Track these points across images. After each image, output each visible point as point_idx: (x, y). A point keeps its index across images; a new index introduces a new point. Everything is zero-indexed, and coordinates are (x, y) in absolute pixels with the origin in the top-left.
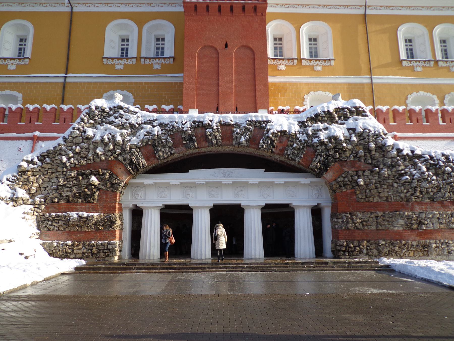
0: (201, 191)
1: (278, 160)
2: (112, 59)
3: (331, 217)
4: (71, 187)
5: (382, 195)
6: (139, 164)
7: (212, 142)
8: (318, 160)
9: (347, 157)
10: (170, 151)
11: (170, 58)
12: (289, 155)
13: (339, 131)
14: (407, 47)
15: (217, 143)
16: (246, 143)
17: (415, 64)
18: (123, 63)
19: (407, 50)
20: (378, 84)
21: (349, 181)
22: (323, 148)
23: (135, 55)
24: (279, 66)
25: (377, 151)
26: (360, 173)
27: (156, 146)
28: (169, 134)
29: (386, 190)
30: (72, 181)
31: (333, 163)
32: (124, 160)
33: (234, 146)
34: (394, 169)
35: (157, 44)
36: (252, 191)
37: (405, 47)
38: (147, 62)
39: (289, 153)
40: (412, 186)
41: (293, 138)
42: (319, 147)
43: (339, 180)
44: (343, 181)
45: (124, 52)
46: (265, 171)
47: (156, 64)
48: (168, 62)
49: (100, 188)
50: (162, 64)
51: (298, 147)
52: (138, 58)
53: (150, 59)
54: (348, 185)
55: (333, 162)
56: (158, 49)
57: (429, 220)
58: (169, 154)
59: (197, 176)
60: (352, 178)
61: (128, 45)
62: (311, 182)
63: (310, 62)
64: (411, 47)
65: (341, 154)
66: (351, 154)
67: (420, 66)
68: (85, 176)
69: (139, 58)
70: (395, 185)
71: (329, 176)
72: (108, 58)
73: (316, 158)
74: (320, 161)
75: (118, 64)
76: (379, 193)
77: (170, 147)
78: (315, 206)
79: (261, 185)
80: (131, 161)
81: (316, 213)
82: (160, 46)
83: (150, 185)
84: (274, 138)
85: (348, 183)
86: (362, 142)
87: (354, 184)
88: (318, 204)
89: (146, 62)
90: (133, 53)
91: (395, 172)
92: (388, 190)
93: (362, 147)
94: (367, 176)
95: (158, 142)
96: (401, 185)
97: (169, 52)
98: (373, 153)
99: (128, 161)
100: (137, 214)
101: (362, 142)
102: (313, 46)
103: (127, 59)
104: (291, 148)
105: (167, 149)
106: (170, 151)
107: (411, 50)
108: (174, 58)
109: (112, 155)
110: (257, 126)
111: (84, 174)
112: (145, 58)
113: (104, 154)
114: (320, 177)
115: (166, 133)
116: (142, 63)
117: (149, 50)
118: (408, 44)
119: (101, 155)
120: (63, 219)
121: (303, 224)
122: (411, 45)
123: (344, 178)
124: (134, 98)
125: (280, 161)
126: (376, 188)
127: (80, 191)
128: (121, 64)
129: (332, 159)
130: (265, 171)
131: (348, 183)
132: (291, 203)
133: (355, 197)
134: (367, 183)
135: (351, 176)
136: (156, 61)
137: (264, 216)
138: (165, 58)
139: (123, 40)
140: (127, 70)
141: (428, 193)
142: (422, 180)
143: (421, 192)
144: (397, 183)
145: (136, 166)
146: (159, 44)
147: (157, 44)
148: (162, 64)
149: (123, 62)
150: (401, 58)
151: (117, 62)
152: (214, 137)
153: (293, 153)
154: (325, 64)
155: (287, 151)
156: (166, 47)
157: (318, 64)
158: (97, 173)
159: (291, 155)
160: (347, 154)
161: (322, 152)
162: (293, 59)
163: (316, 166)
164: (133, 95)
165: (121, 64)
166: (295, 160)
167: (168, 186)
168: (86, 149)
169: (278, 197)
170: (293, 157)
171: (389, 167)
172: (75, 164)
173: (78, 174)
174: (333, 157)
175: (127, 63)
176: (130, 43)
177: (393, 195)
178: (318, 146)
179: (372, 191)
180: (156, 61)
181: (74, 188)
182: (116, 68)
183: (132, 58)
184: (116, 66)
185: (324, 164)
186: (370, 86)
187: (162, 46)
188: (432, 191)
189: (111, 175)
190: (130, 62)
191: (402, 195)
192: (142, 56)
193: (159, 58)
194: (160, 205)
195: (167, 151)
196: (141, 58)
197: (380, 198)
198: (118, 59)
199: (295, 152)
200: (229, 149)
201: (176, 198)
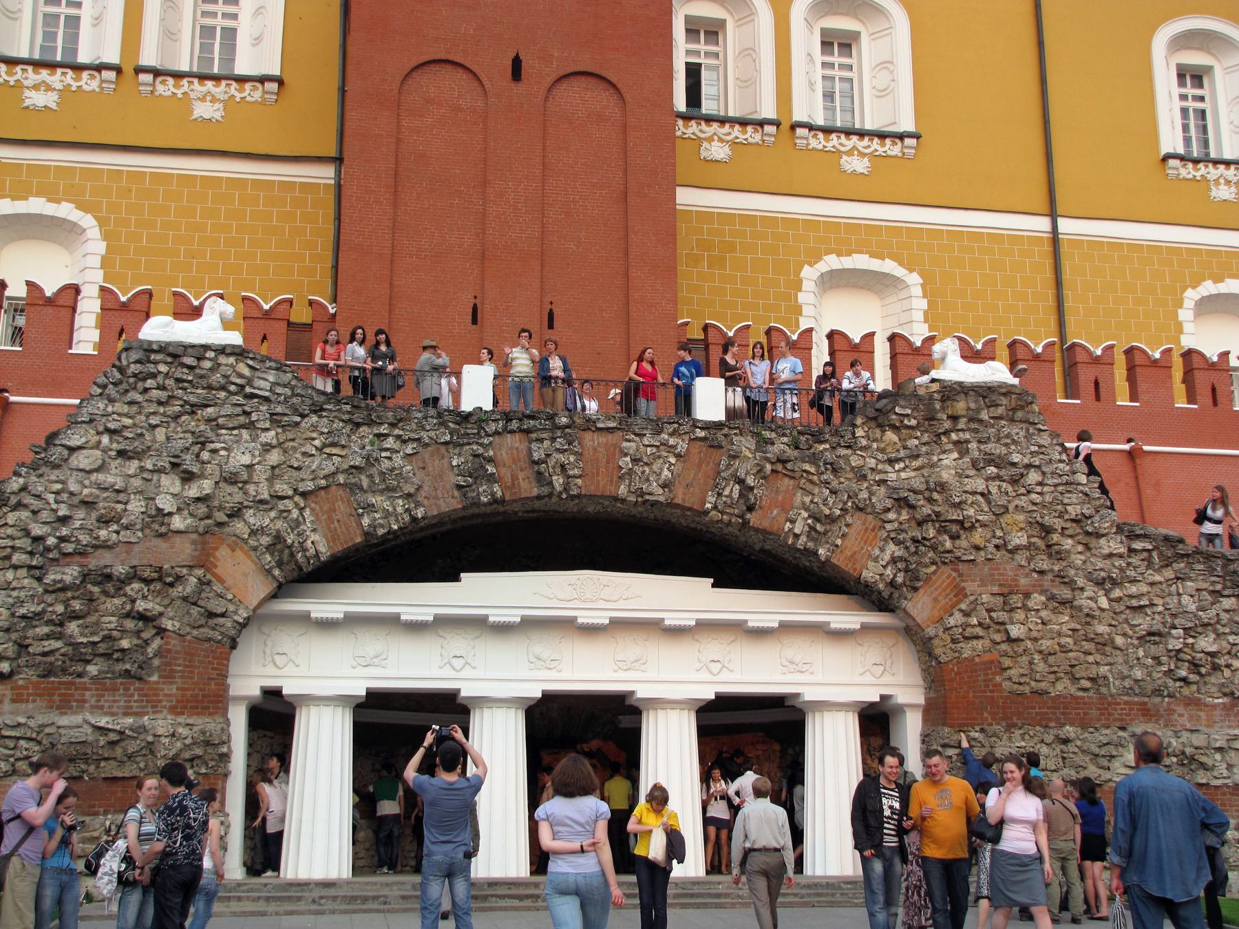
0: (499, 647)
1: (757, 547)
3: (923, 742)
4: (61, 624)
5: (1079, 672)
6: (305, 550)
7: (551, 483)
8: (887, 557)
9: (977, 548)
10: (408, 510)
11: (262, 80)
12: (797, 536)
14: (1185, 104)
15: (566, 489)
16: (661, 491)
17: (1213, 172)
18: (59, 86)
19: (1184, 111)
20: (1077, 243)
21: (980, 624)
22: (905, 516)
23: (113, 58)
24: (705, 144)
25: (1067, 532)
26: (1016, 600)
27: (361, 488)
28: (409, 451)
29: (1091, 659)
30: (66, 603)
31: (934, 568)
32: (253, 533)
33: (623, 501)
34: (1117, 593)
35: (204, 14)
36: (672, 649)
37: (1178, 104)
38: (166, 88)
39: (797, 531)
40: (1170, 647)
41: (811, 482)
42: (891, 516)
43: (952, 621)
44: (965, 626)
46: (714, 586)
47: (203, 99)
48: (257, 95)
49: (165, 630)
50: (229, 103)
51: (827, 512)
53: (178, 76)
54: (977, 637)
55: (933, 563)
56: (207, 32)
57: (1218, 756)
58: (407, 518)
59: (482, 591)
60: (991, 618)
62: (865, 628)
63: (827, 140)
64: (1199, 105)
65: (958, 537)
66: (989, 541)
67: (1228, 182)
68: (110, 587)
69: (128, 70)
70: (1119, 641)
71: (920, 607)
73: (882, 550)
74: (894, 560)
75: (36, 87)
76: (1072, 666)
77: (409, 495)
78: (872, 705)
79: (706, 627)
80: (278, 538)
81: (876, 723)
82: (220, 22)
83: (327, 625)
84: (750, 481)
85: (979, 631)
86: (1023, 502)
87: (998, 637)
88: (883, 697)
89: (160, 89)
91: (1119, 600)
92: (1098, 658)
93: (1021, 517)
94: (1038, 610)
95: (371, 476)
96: (1136, 642)
97: (259, 52)
98: (1055, 537)
99: (265, 540)
100: (274, 721)
101: (1023, 502)
102: (837, 73)
104: (806, 515)
105: (400, 502)
106: (408, 510)
107: (1202, 114)
108: (280, 81)
109: (208, 517)
110: (697, 439)
111: (109, 577)
112: (157, 73)
113: (179, 510)
114: (892, 611)
115: (397, 446)
118: (1190, 91)
119: (170, 514)
120: (34, 735)
121: (833, 761)
122: (1202, 99)
123: (967, 614)
124: (106, 237)
125: (762, 551)
126: (1065, 650)
127: (96, 639)
128: (49, 88)
129: (931, 554)
130: (714, 586)
131: (979, 631)
132: (797, 695)
133: (998, 679)
134: (1034, 634)
135: (989, 611)
136: (204, 89)
137: (705, 733)
138: (242, 80)
141: (1216, 668)
142: (1200, 629)
143: (1195, 666)
144: (1125, 635)
145: (292, 555)
146: (214, 15)
147: (204, 14)
148: (229, 103)
149: (56, 79)
150: (1165, 149)
151: (32, 76)
152: (558, 470)
153: (812, 528)
154: (881, 150)
155: (793, 522)
157: (854, 148)
158: (155, 575)
159: (803, 539)
160: (978, 536)
161: (900, 531)
162: (761, 123)
163: (881, 575)
164: (101, 222)
165: (49, 88)
166: (815, 554)
167: (391, 622)
168: (118, 491)
169: (754, 673)
170: (810, 545)
171: (1100, 583)
172: (78, 541)
173: (85, 576)
174: (934, 548)
175: (75, 85)
177: (1110, 671)
178: (889, 510)
179: (1051, 659)
180: (204, 89)
181: (73, 627)
182: (28, 102)
183: (100, 68)
184: (27, 93)
185: (906, 571)
186: (1047, 248)
187: (230, 23)
188: (1228, 666)
189: (204, 583)
190: (89, 82)
191: (1138, 674)
193: (217, 79)
194: (359, 689)
195: (400, 510)
196: (139, 70)
197: (1075, 680)
198: (37, 64)
199: (819, 527)
200: (599, 507)
201: (413, 667)
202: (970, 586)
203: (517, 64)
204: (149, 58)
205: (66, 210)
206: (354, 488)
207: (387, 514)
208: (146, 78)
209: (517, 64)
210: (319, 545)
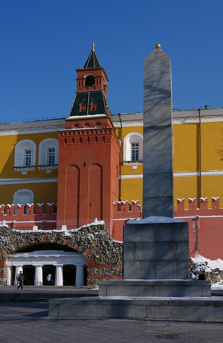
2: (20, 167)
13: (90, 236)
23: (34, 164)
38: (42, 168)
45: (28, 160)
52: (36, 166)
56: (50, 157)
59: (36, 254)
61: (30, 155)
72: (17, 167)
82: (52, 155)
90: (33, 163)
103: (29, 167)
116: (39, 169)
117: (43, 160)
139: (27, 152)
140: (30, 175)
149: (27, 169)
151: (22, 169)
156: (55, 155)
176: (31, 154)
190: (31, 169)
192: (39, 165)
196: (38, 166)
202: (92, 251)
203: (85, 163)
204: (40, 164)
205: (28, 190)
206: (17, 242)
207: (21, 245)
208: (39, 167)
209: (85, 163)
210: (14, 249)
